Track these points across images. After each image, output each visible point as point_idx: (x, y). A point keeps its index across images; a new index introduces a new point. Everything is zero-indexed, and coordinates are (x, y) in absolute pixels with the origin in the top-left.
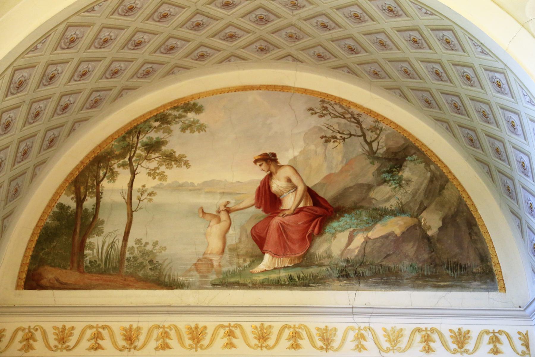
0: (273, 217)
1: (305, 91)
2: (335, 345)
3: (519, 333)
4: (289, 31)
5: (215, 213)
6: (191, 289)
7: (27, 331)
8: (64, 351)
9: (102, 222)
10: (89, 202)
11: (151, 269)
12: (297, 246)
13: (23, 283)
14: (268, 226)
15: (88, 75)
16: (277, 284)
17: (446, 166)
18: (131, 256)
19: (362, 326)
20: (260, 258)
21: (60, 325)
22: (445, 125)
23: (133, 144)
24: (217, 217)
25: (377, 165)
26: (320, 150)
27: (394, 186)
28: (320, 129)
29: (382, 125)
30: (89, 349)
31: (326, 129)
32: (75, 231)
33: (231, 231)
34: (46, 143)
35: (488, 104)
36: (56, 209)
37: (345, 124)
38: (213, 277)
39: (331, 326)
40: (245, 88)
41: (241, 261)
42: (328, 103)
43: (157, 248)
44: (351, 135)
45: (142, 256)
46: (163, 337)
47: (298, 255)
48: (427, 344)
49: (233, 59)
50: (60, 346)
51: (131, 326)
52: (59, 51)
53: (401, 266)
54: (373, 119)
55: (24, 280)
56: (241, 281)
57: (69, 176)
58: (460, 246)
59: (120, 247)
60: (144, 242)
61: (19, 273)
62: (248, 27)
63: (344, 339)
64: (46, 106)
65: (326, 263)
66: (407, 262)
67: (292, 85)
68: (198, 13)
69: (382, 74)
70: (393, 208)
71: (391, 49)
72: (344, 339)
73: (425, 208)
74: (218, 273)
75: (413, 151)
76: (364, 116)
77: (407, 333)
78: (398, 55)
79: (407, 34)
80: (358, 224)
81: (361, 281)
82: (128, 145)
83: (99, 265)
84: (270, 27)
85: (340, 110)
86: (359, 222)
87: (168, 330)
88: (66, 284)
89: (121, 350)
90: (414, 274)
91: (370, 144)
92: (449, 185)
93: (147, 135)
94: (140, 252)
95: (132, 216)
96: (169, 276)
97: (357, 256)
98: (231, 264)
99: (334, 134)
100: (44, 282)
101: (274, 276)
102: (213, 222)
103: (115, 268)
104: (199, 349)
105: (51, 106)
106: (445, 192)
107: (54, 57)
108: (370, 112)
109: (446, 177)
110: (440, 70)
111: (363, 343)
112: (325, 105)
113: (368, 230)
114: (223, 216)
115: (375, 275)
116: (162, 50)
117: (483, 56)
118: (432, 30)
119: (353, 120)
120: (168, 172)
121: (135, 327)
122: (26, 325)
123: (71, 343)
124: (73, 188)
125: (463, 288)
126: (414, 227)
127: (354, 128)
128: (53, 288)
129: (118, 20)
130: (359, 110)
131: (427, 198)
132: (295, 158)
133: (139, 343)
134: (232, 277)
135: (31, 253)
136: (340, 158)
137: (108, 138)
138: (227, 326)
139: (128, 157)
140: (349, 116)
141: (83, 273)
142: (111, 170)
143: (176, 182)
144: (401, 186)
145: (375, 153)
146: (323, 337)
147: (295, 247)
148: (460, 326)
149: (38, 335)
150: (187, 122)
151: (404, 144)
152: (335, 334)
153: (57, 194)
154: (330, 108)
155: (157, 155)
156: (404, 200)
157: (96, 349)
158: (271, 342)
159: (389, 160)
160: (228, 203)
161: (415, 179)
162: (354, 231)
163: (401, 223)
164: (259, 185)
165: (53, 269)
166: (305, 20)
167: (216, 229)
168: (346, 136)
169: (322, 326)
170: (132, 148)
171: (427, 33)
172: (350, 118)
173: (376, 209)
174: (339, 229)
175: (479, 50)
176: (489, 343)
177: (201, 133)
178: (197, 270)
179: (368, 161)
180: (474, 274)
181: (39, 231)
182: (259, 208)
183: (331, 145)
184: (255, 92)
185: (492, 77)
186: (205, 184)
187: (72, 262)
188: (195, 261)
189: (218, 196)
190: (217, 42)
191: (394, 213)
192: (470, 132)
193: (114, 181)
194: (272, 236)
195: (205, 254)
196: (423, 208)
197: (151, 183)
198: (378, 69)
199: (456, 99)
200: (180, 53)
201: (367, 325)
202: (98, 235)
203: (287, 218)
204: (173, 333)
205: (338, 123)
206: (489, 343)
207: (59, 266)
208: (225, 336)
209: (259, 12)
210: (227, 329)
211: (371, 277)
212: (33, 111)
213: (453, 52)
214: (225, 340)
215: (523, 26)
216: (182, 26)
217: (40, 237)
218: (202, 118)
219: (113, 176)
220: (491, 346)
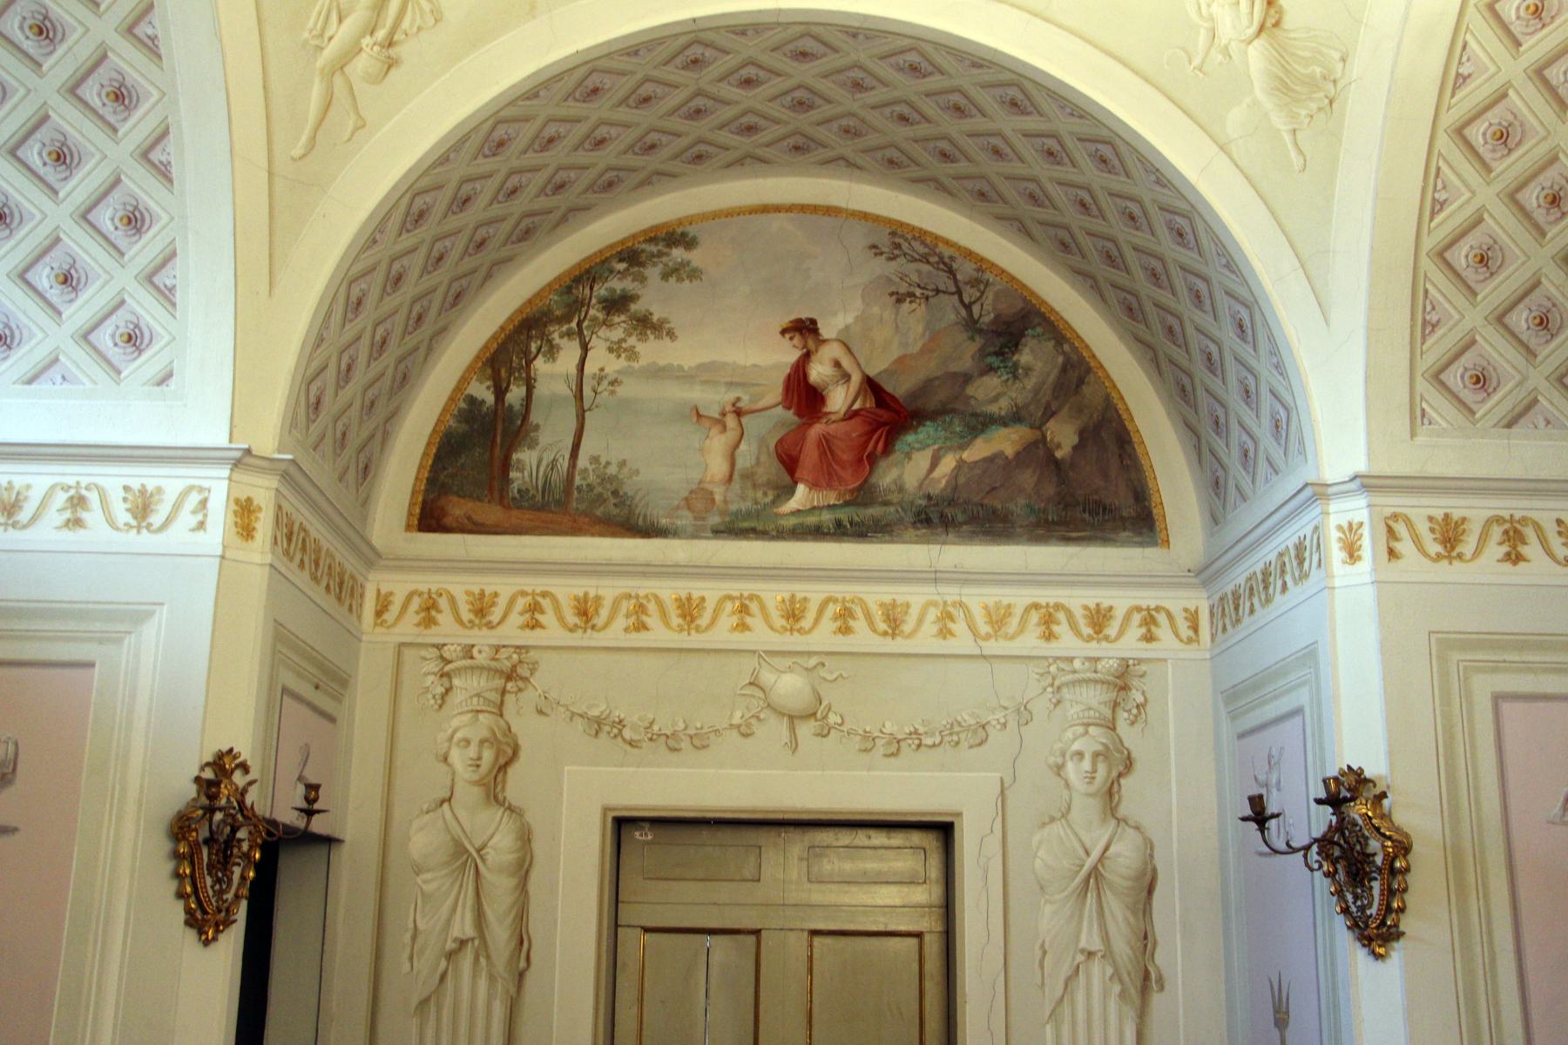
0: (811, 425)
1: (865, 216)
2: (907, 628)
3: (1186, 610)
4: (844, 122)
5: (717, 416)
6: (680, 538)
7: (426, 596)
8: (485, 629)
9: (537, 427)
10: (515, 394)
11: (615, 505)
12: (850, 471)
13: (416, 522)
14: (804, 439)
15: (518, 194)
16: (817, 533)
17: (1087, 346)
18: (584, 483)
19: (949, 599)
20: (791, 491)
21: (476, 590)
22: (1090, 282)
23: (584, 299)
24: (720, 423)
25: (979, 341)
26: (888, 314)
27: (1005, 377)
28: (889, 280)
29: (989, 276)
30: (522, 628)
31: (898, 280)
32: (494, 441)
33: (743, 447)
34: (450, 299)
35: (1161, 259)
36: (463, 405)
37: (930, 272)
38: (714, 520)
39: (900, 599)
40: (765, 209)
41: (759, 494)
42: (902, 236)
43: (625, 470)
44: (938, 291)
45: (600, 484)
46: (637, 613)
47: (851, 487)
48: (1048, 628)
49: (748, 161)
50: (477, 621)
51: (586, 594)
52: (481, 160)
53: (1012, 507)
54: (974, 266)
56: (760, 527)
57: (481, 350)
58: (1105, 476)
59: (565, 469)
60: (603, 461)
62: (777, 114)
63: (920, 621)
64: (453, 245)
65: (895, 501)
66: (1022, 501)
67: (843, 205)
68: (698, 95)
69: (994, 196)
70: (1003, 413)
71: (1010, 161)
72: (920, 621)
73: (1053, 414)
74: (723, 513)
75: (1037, 320)
76: (960, 260)
77: (1018, 611)
78: (1019, 169)
79: (1039, 141)
80: (946, 438)
81: (950, 529)
82: (576, 301)
83: (534, 496)
84: (814, 115)
85: (922, 250)
86: (948, 434)
87: (644, 602)
88: (482, 525)
89: (571, 630)
90: (1033, 519)
91: (968, 307)
92: (1091, 378)
93: (606, 285)
94: (598, 476)
95: (583, 418)
96: (645, 516)
97: (944, 489)
98: (743, 498)
99: (912, 289)
100: (448, 521)
101: (811, 520)
102: (715, 431)
103: (558, 503)
104: (693, 632)
105: (461, 242)
106: (1086, 390)
107: (473, 170)
108: (969, 254)
109: (1088, 363)
110: (1088, 199)
111: (950, 625)
112: (897, 240)
113: (963, 447)
114: (731, 421)
115: (973, 520)
116: (637, 150)
117: (1158, 188)
118: (1080, 139)
119: (941, 266)
120: (640, 348)
121: (592, 594)
122: (423, 588)
123: (495, 616)
124: (489, 371)
125: (1106, 541)
126: (1035, 444)
127: (943, 281)
128: (462, 530)
129: (574, 109)
130: (952, 250)
131: (1056, 398)
132: (847, 328)
133: (599, 621)
134: (744, 520)
135: (426, 475)
136: (920, 329)
137: (542, 290)
138: (737, 598)
139: (576, 320)
140: (934, 259)
141: (507, 508)
142: (550, 342)
143: (654, 363)
144: (1016, 377)
145: (976, 322)
146: (888, 616)
147: (847, 474)
148: (1098, 600)
149: (443, 603)
150: (671, 264)
151: (1023, 309)
152: (906, 613)
153: (464, 380)
154: (905, 246)
155: (623, 318)
156: (1020, 402)
157: (533, 628)
158: (806, 623)
159: (998, 334)
160: (738, 399)
161: (1038, 366)
162: (940, 449)
163: (1015, 437)
164: (788, 371)
165: (462, 501)
166: (874, 108)
167: (718, 444)
168: (930, 294)
169: (887, 599)
170: (583, 306)
171: (1070, 143)
172: (938, 263)
173: (975, 415)
174: (917, 445)
175: (1153, 178)
176: (1141, 626)
177: (695, 282)
178: (689, 508)
179: (965, 335)
180: (1123, 519)
182: (788, 408)
183: (906, 306)
184: (782, 215)
185: (1170, 221)
186: (702, 367)
187: (491, 489)
188: (686, 494)
189: (723, 389)
190: (724, 137)
191: (1004, 422)
192: (1128, 296)
193: (554, 360)
194: (810, 455)
195: (701, 482)
196: (1049, 414)
197: (614, 365)
198: (986, 188)
199: (1110, 245)
200: (664, 153)
201: (957, 598)
202: (530, 447)
203: (833, 426)
204: (652, 607)
205: (918, 272)
206: (1141, 626)
207: (471, 497)
208: (733, 613)
209: (798, 94)
210: (737, 603)
211: (965, 523)
213: (1112, 176)
214: (734, 620)
215: (1222, 148)
216: (672, 112)
217: (439, 450)
218: (695, 257)
219: (552, 351)
220: (1143, 630)
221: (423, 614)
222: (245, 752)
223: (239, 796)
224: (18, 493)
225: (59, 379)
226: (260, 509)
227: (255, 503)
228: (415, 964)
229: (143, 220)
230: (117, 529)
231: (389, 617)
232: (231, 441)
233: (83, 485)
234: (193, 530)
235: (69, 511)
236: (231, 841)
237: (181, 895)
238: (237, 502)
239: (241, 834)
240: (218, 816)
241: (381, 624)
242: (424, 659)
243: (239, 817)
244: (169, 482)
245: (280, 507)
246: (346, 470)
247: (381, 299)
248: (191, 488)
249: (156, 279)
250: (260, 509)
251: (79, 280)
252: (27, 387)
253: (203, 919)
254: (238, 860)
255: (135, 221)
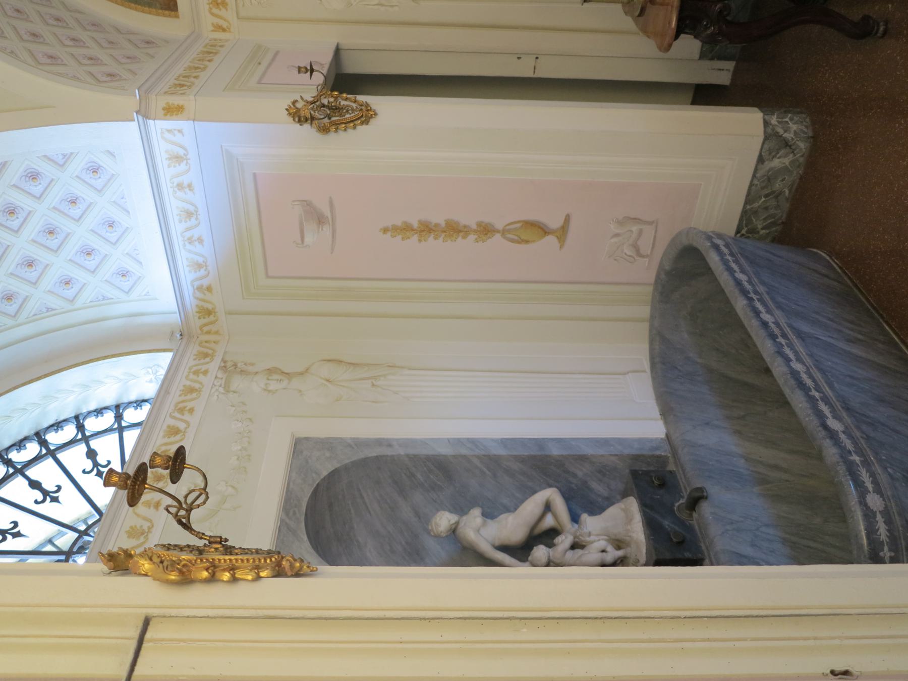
7: (211, 6)
13: (173, 13)
55: (170, 12)
61: (165, 17)
122: (207, 7)
181: (126, 3)
212: (15, 14)
221: (221, 7)
222: (289, 102)
223: (309, 104)
224: (181, 211)
225: (124, 200)
226: (168, 103)
227: (165, 106)
228: (394, 4)
229: (31, 172)
230: (189, 169)
231: (225, 25)
232: (134, 121)
233: (172, 185)
234: (183, 135)
235: (185, 190)
236: (330, 108)
237: (355, 127)
238: (165, 115)
239: (326, 103)
240: (317, 115)
241: (229, 29)
242: (243, 5)
243: (317, 103)
244: (161, 149)
245: (165, 93)
246: (148, 54)
247: (48, 44)
248: (163, 138)
249: (61, 163)
250: (168, 103)
251: (71, 197)
252: (131, 212)
253: (365, 116)
254: (338, 103)
255: (34, 176)
